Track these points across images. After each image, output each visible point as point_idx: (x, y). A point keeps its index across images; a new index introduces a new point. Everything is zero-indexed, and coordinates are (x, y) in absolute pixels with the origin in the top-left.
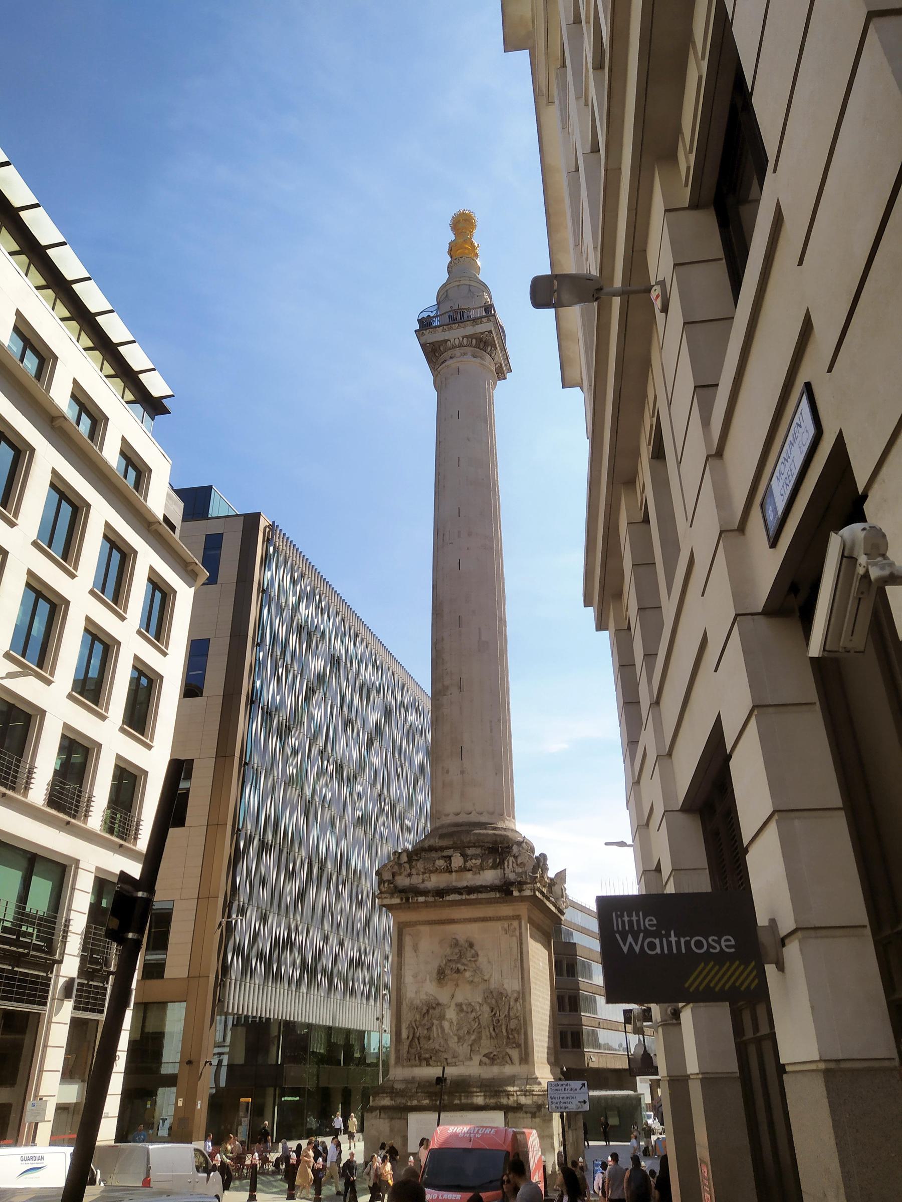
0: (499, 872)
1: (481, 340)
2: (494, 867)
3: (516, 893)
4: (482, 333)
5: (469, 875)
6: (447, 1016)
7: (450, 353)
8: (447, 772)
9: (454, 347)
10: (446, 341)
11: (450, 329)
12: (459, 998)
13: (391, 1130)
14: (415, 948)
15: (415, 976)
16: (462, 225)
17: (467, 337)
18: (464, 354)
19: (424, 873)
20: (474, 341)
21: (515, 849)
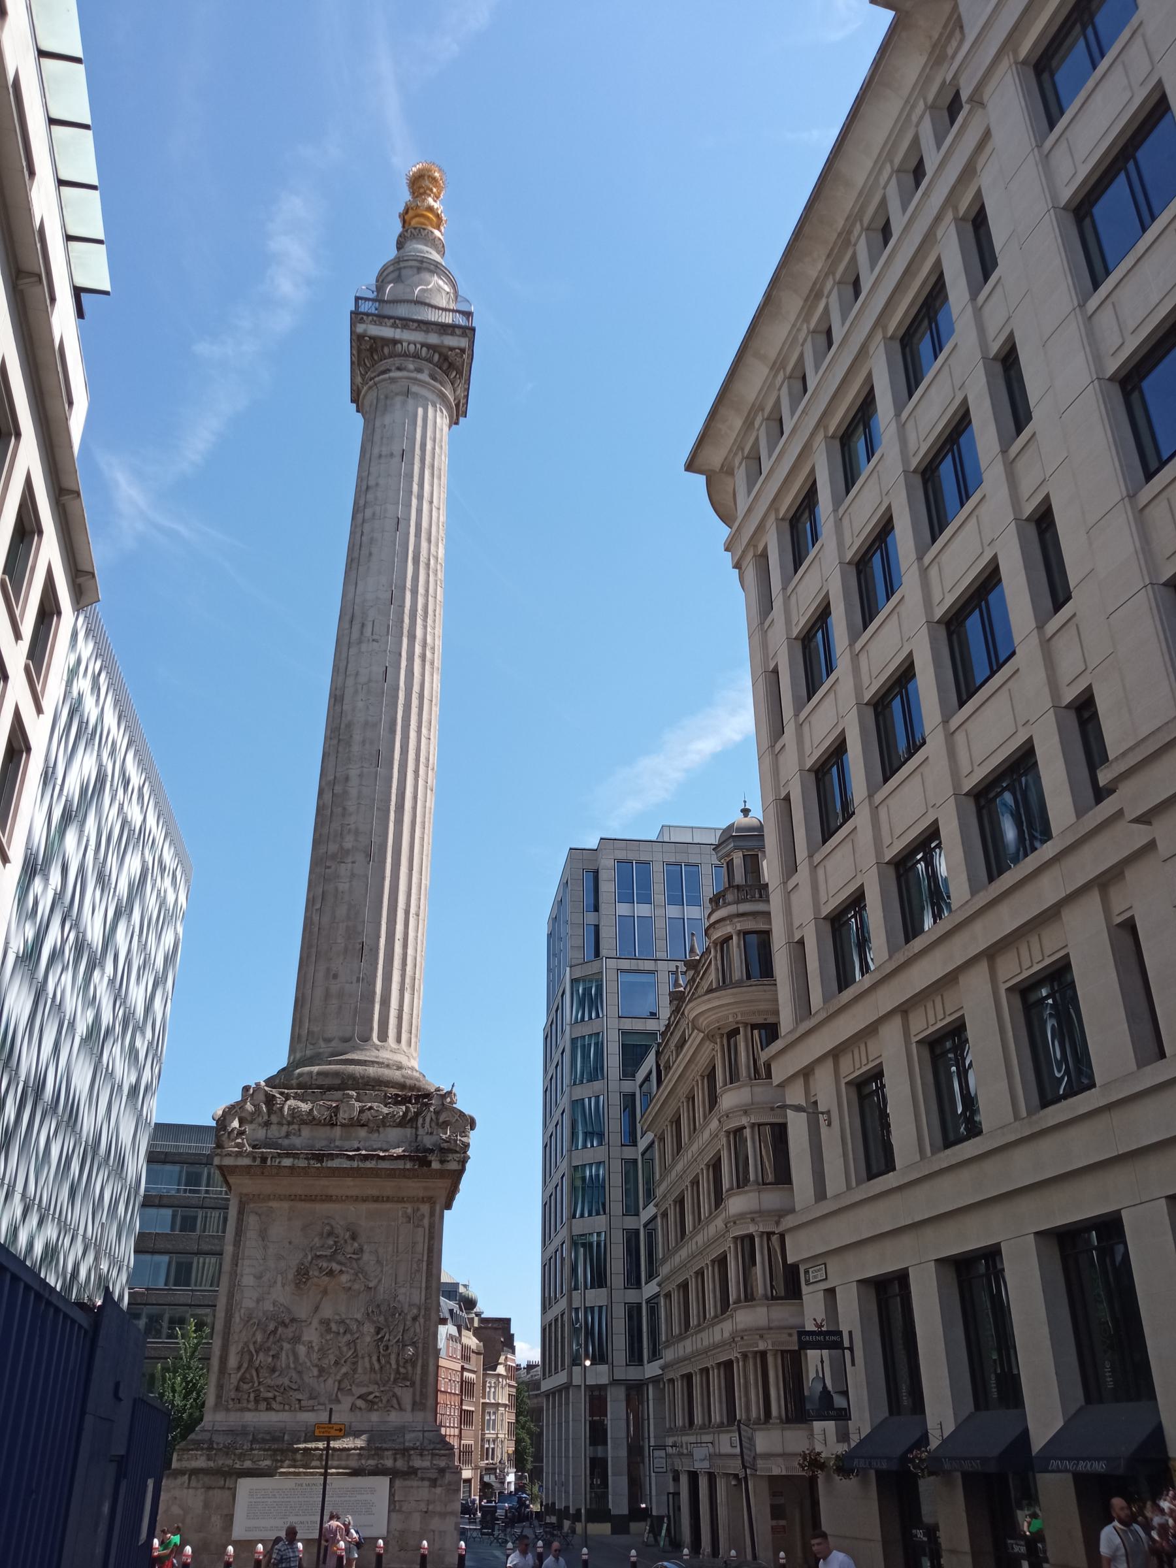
1: (446, 358)
3: (435, 1165)
4: (452, 349)
6: (305, 1338)
7: (398, 361)
8: (335, 976)
9: (406, 355)
10: (395, 342)
11: (381, 324)
12: (327, 1312)
13: (206, 1505)
14: (263, 1235)
15: (259, 1277)
17: (429, 347)
19: (289, 1124)
20: (436, 357)
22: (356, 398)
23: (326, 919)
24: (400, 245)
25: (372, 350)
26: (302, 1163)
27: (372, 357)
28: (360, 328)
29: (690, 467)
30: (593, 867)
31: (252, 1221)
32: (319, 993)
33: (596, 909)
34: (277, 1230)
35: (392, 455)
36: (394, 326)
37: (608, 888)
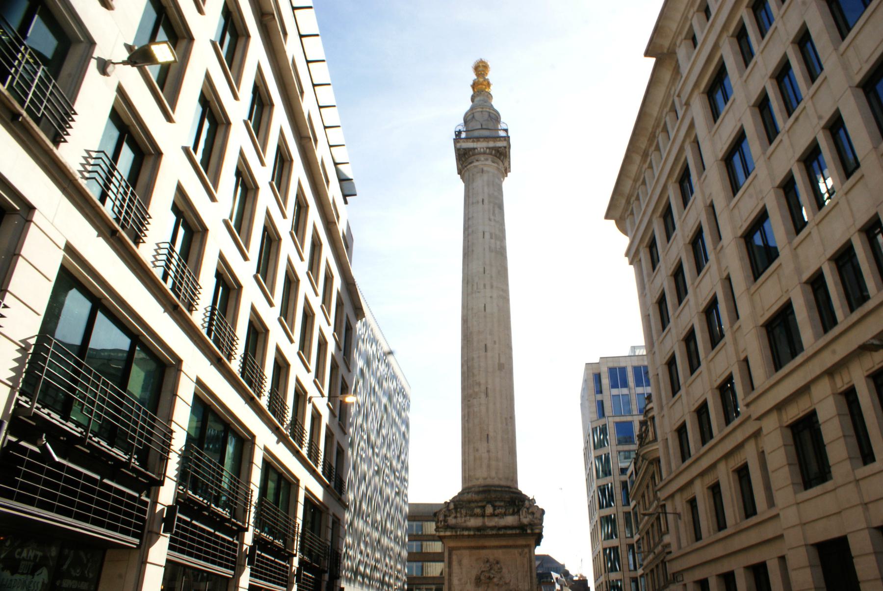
0: (516, 517)
2: (513, 514)
3: (529, 531)
5: (496, 519)
7: (476, 157)
8: (477, 450)
9: (480, 154)
10: (474, 149)
15: (460, 580)
16: (481, 69)
17: (489, 148)
18: (487, 160)
21: (527, 502)
22: (460, 172)
23: (471, 425)
24: (473, 100)
25: (465, 154)
26: (472, 533)
27: (464, 158)
28: (458, 145)
29: (608, 216)
30: (597, 372)
31: (454, 557)
32: (472, 458)
33: (601, 392)
34: (465, 561)
35: (478, 202)
36: (473, 142)
37: (606, 381)
